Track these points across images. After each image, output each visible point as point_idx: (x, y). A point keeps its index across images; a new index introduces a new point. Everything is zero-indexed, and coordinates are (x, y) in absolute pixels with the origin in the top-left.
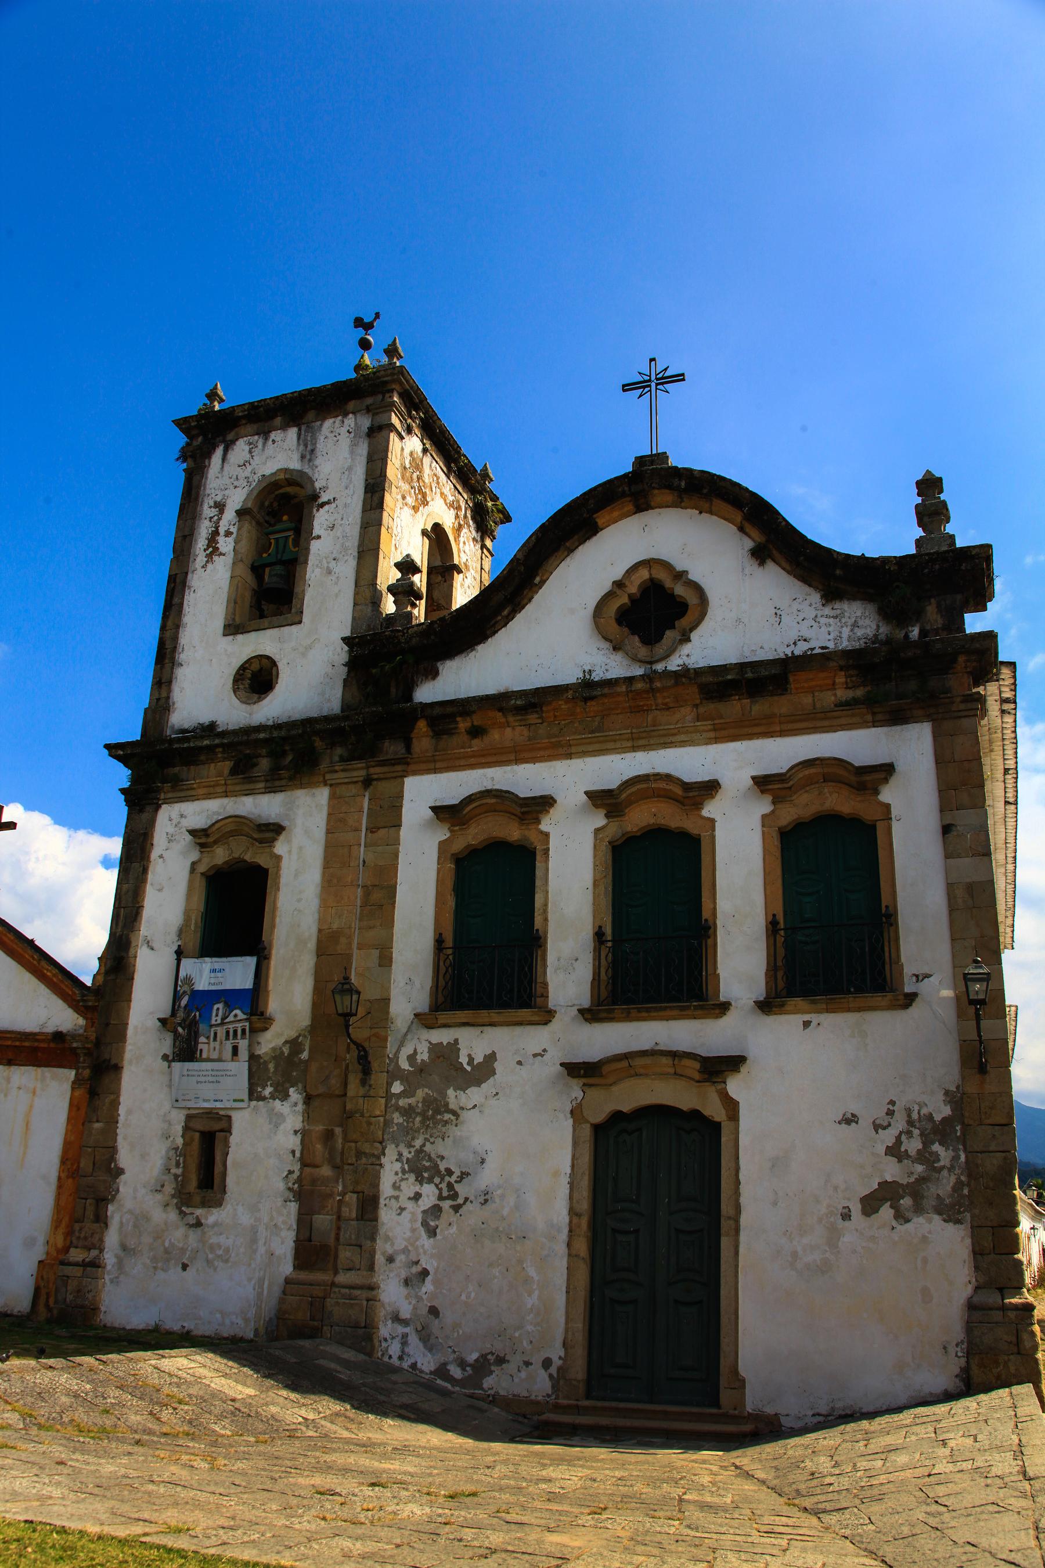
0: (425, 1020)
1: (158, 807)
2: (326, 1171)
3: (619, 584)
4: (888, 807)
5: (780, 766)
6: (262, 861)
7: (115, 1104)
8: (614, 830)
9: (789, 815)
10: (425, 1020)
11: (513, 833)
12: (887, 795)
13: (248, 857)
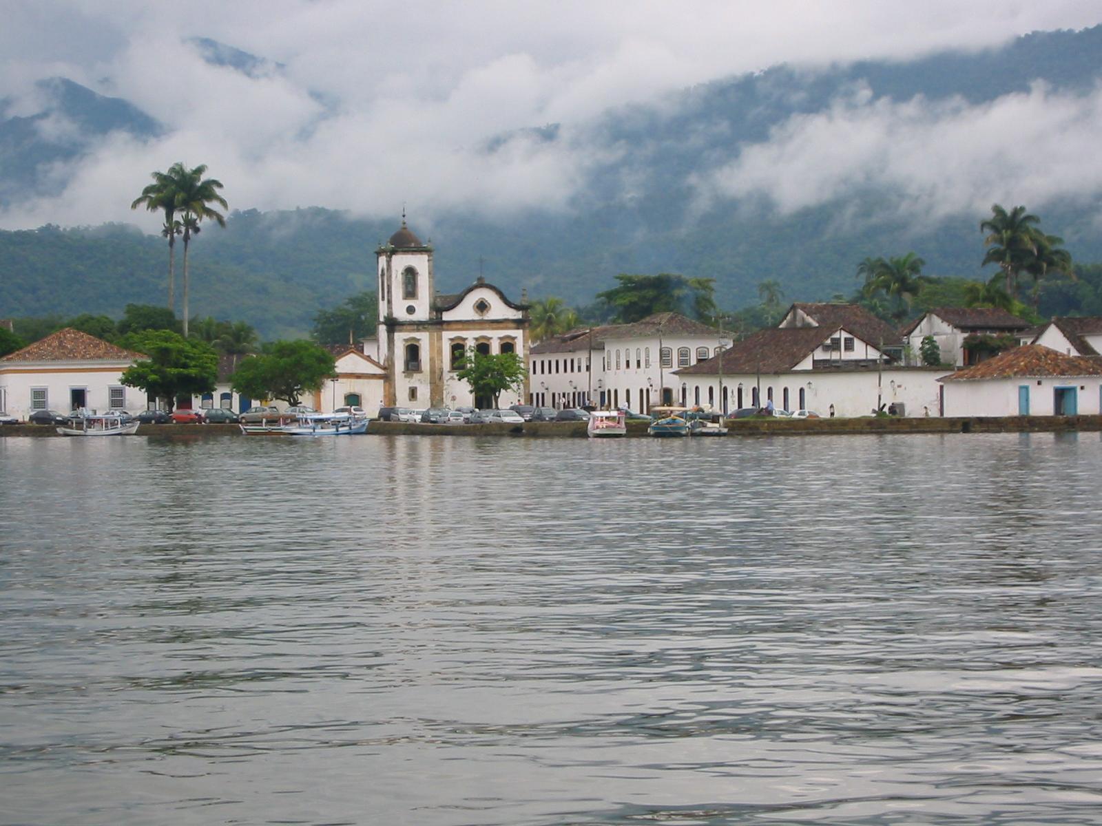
0: (449, 372)
1: (394, 332)
2: (434, 394)
3: (477, 301)
4: (516, 343)
5: (502, 336)
6: (417, 344)
7: (395, 385)
8: (477, 343)
9: (502, 342)
10: (449, 372)
11: (461, 342)
12: (516, 340)
13: (415, 343)
